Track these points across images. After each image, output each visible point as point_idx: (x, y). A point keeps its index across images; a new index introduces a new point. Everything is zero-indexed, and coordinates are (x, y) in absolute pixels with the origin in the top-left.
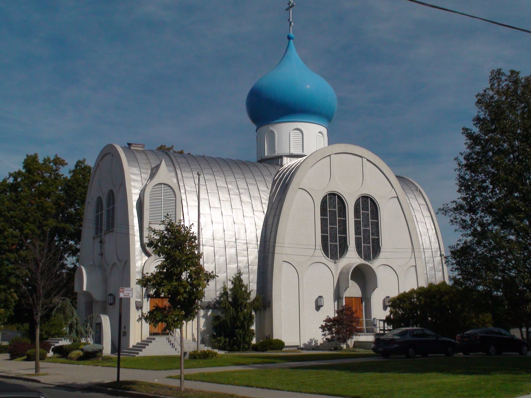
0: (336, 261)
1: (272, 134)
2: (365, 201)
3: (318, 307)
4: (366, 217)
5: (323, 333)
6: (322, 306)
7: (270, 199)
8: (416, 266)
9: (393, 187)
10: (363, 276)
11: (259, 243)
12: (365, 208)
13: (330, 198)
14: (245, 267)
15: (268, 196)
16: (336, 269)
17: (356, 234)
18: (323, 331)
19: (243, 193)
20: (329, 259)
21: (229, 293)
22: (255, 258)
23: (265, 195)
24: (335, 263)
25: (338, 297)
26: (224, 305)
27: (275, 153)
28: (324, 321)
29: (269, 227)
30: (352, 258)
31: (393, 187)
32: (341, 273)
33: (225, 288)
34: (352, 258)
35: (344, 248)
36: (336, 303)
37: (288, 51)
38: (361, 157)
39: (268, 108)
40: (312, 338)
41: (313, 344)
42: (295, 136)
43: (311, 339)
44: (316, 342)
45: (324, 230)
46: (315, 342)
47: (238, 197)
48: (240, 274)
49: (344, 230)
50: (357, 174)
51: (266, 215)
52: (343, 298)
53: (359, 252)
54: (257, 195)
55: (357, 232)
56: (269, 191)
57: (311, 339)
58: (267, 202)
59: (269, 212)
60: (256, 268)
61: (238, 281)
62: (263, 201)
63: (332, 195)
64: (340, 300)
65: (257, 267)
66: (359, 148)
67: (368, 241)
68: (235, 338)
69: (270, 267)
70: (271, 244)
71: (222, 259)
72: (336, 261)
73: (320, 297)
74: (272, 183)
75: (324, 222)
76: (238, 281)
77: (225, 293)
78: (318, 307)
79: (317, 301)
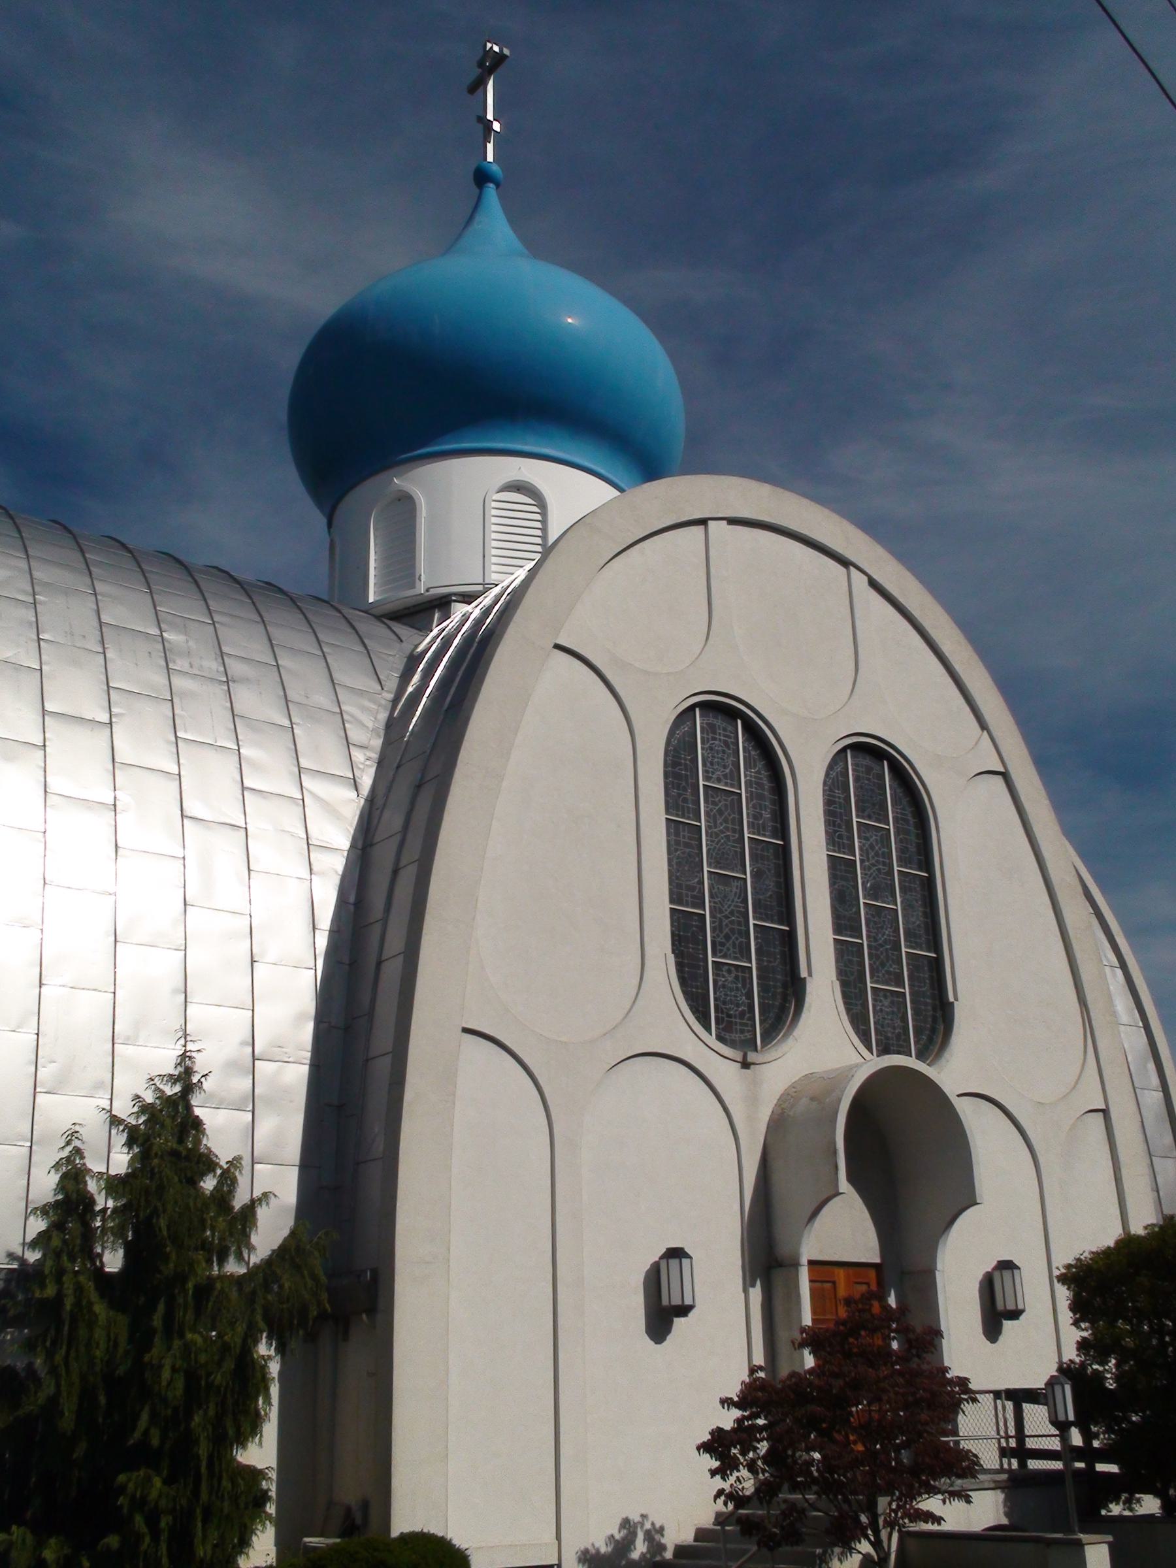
0: (752, 1057)
1: (406, 504)
2: (869, 770)
3: (662, 1315)
4: (877, 843)
5: (718, 1483)
6: (684, 1310)
7: (394, 727)
8: (1105, 1112)
9: (983, 726)
10: (900, 1148)
11: (322, 941)
12: (872, 805)
13: (709, 729)
14: (232, 1066)
15: (383, 716)
16: (753, 1100)
17: (838, 928)
18: (721, 1472)
19: (245, 680)
20: (712, 1040)
21: (104, 1202)
22: (300, 1018)
23: (363, 709)
24: (746, 1065)
25: (766, 1259)
26: (50, 1291)
27: (412, 585)
28: (726, 1402)
29: (384, 855)
30: (824, 1047)
31: (983, 726)
32: (778, 1124)
33: (73, 1175)
34: (824, 1047)
35: (786, 996)
36: (756, 1293)
37: (477, 218)
38: (845, 563)
39: (382, 401)
40: (635, 1517)
41: (640, 1548)
42: (505, 519)
43: (625, 1523)
44: (654, 1536)
45: (682, 888)
46: (649, 1536)
47: (211, 628)
48: (186, 1076)
49: (781, 901)
50: (827, 636)
51: (371, 800)
52: (796, 1265)
53: (858, 1021)
54: (323, 699)
55: (844, 921)
56: (390, 696)
57: (625, 1523)
58: (377, 743)
59: (381, 791)
60: (297, 1075)
61: (167, 1129)
62: (355, 735)
63: (721, 711)
64: (778, 1276)
65: (305, 1070)
66: (835, 518)
67: (894, 968)
68: (113, 1541)
69: (382, 1067)
70: (395, 942)
71: (92, 1006)
72: (752, 1057)
73: (676, 1253)
74: (401, 667)
75: (682, 840)
76: (167, 1129)
77: (71, 1205)
78: (662, 1315)
79: (654, 1280)
